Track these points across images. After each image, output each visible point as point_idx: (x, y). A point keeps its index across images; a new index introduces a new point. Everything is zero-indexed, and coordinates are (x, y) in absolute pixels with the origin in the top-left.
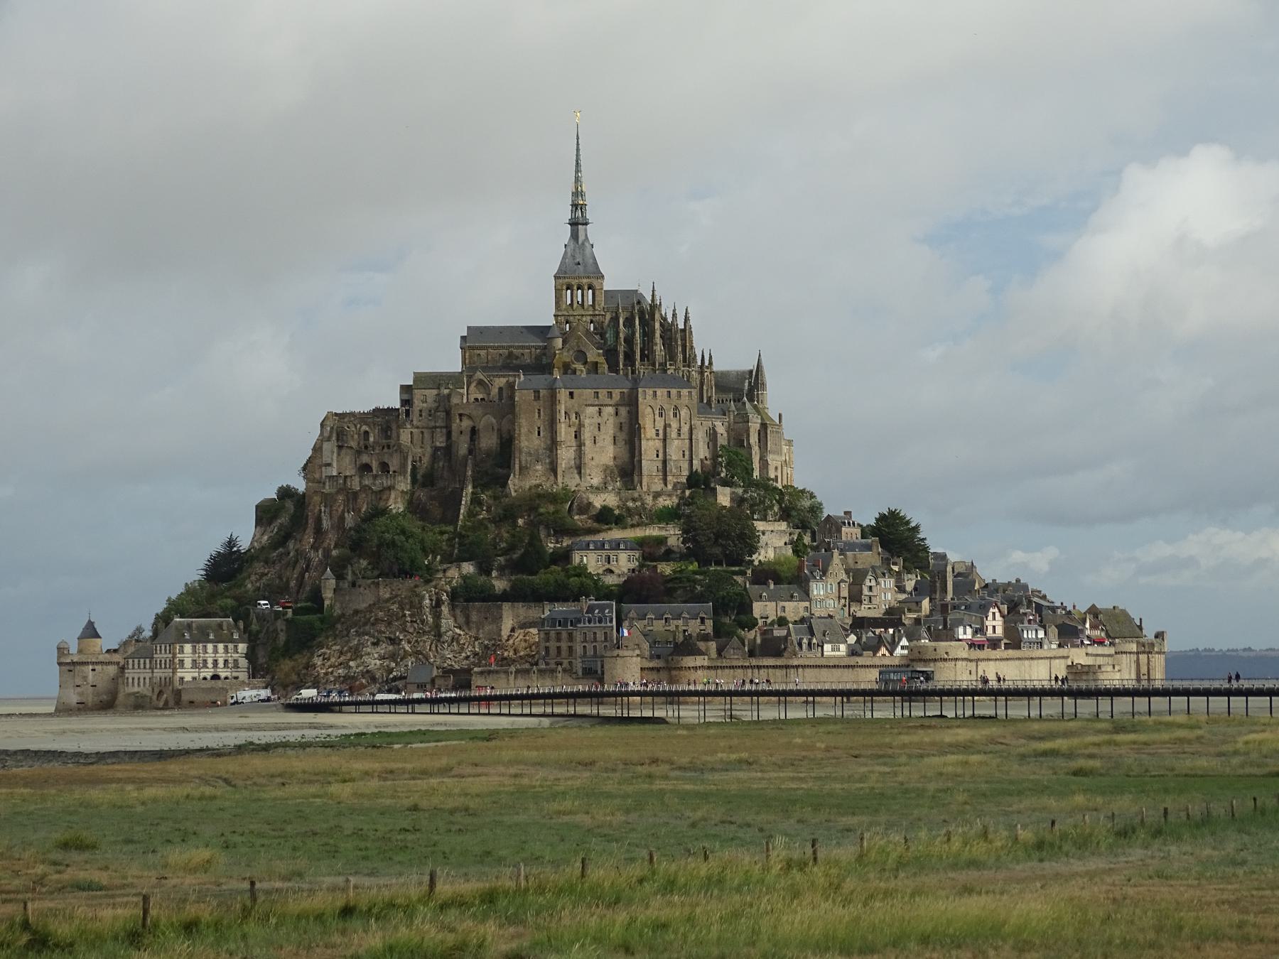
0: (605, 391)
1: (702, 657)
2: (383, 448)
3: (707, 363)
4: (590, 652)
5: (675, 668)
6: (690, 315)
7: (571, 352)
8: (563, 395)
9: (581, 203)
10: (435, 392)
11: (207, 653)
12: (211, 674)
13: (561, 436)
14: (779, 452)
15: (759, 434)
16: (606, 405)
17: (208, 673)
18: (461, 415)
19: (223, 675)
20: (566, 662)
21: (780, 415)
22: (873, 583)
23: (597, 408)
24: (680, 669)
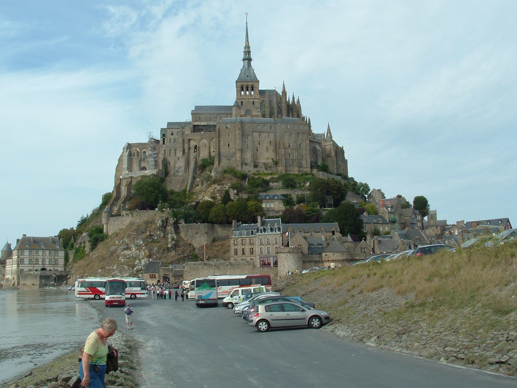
0: (262, 125)
1: (347, 253)
4: (265, 252)
6: (300, 100)
7: (245, 110)
9: (248, 50)
10: (179, 130)
11: (39, 255)
12: (41, 268)
15: (336, 152)
16: (263, 132)
17: (39, 267)
18: (189, 140)
19: (48, 269)
21: (342, 147)
22: (414, 217)
23: (258, 133)
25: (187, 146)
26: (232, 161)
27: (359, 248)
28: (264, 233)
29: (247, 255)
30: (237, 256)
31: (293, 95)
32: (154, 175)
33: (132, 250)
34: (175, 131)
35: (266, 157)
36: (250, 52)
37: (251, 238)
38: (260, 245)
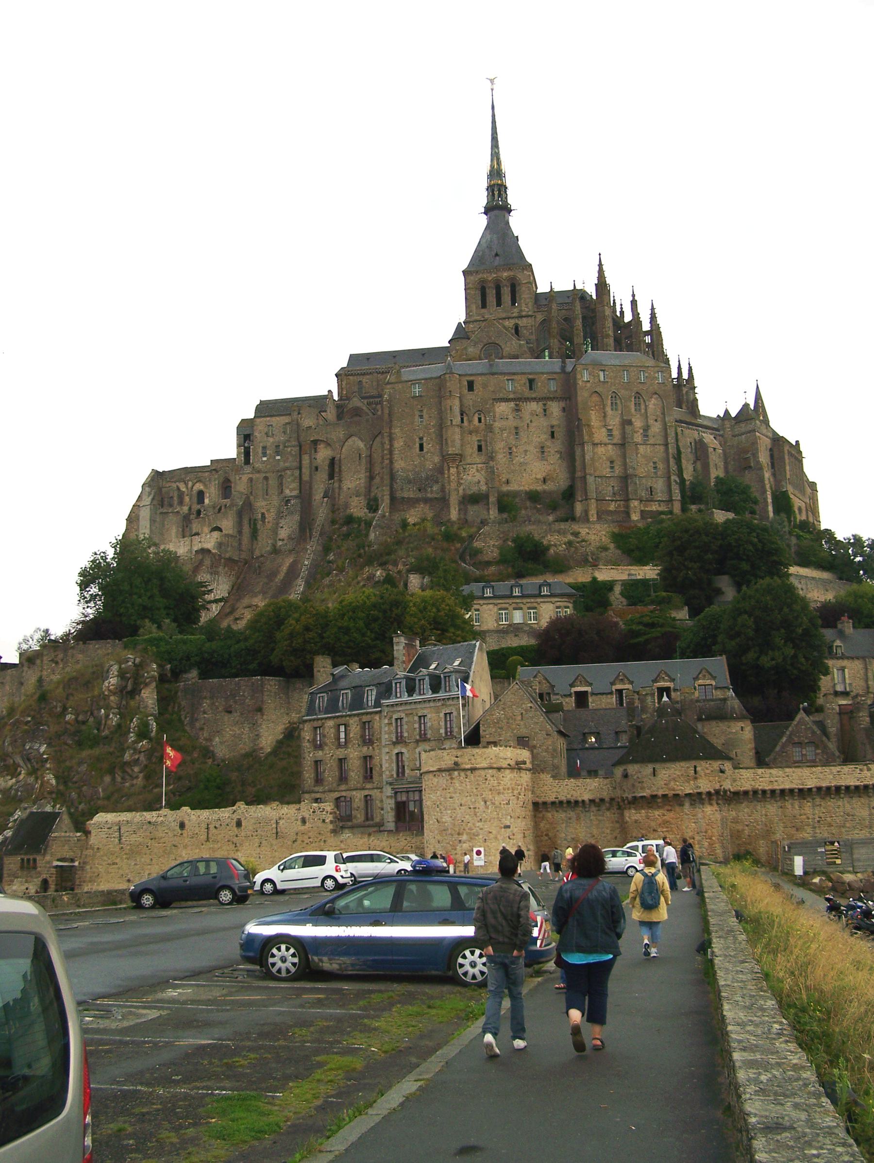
1: (716, 764)
2: (220, 509)
3: (685, 376)
5: (636, 802)
6: (656, 311)
8: (454, 386)
9: (499, 182)
10: (286, 419)
13: (453, 446)
14: (803, 491)
15: (772, 456)
18: (315, 442)
20: (358, 797)
21: (797, 442)
23: (512, 404)
24: (652, 801)
25: (308, 461)
26: (432, 492)
27: (784, 746)
28: (409, 696)
29: (352, 783)
30: (321, 789)
31: (633, 296)
32: (204, 551)
33: (20, 774)
34: (278, 421)
35: (539, 476)
36: (506, 188)
37: (365, 718)
38: (394, 744)
